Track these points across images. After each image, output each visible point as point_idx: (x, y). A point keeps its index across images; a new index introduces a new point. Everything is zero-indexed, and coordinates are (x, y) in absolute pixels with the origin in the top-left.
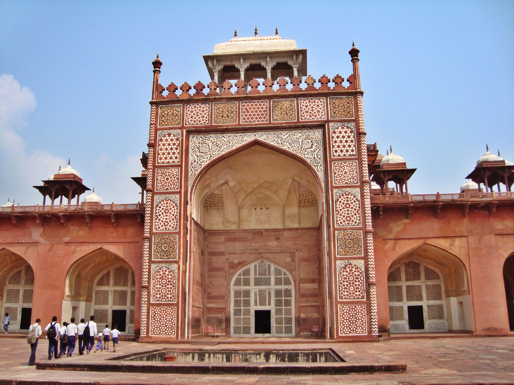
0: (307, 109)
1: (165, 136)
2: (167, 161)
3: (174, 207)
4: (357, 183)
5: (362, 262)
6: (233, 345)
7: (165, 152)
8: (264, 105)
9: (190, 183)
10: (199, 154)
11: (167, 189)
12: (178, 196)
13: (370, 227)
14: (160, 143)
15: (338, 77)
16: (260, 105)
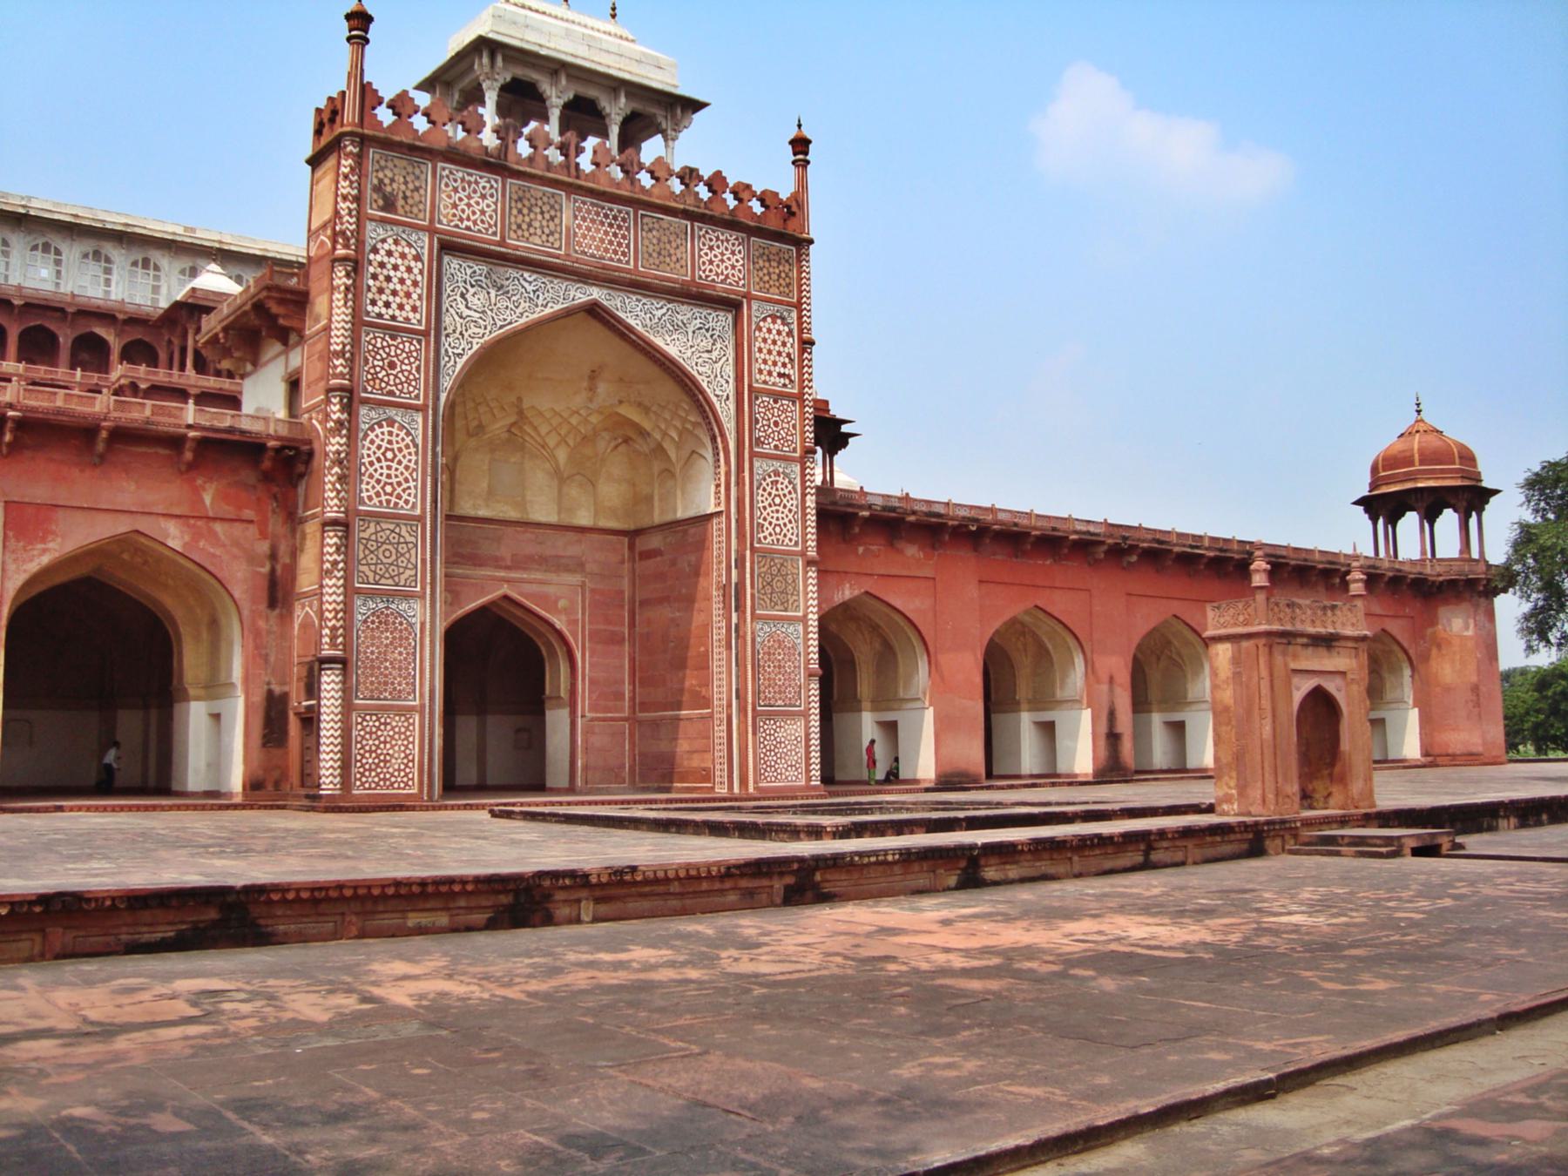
0: (711, 255)
1: (384, 241)
2: (390, 312)
3: (407, 447)
4: (795, 450)
5: (801, 628)
6: (599, 807)
7: (385, 285)
8: (624, 220)
9: (447, 383)
10: (466, 312)
11: (391, 393)
12: (419, 418)
13: (812, 553)
14: (372, 256)
15: (718, 175)
16: (615, 218)
